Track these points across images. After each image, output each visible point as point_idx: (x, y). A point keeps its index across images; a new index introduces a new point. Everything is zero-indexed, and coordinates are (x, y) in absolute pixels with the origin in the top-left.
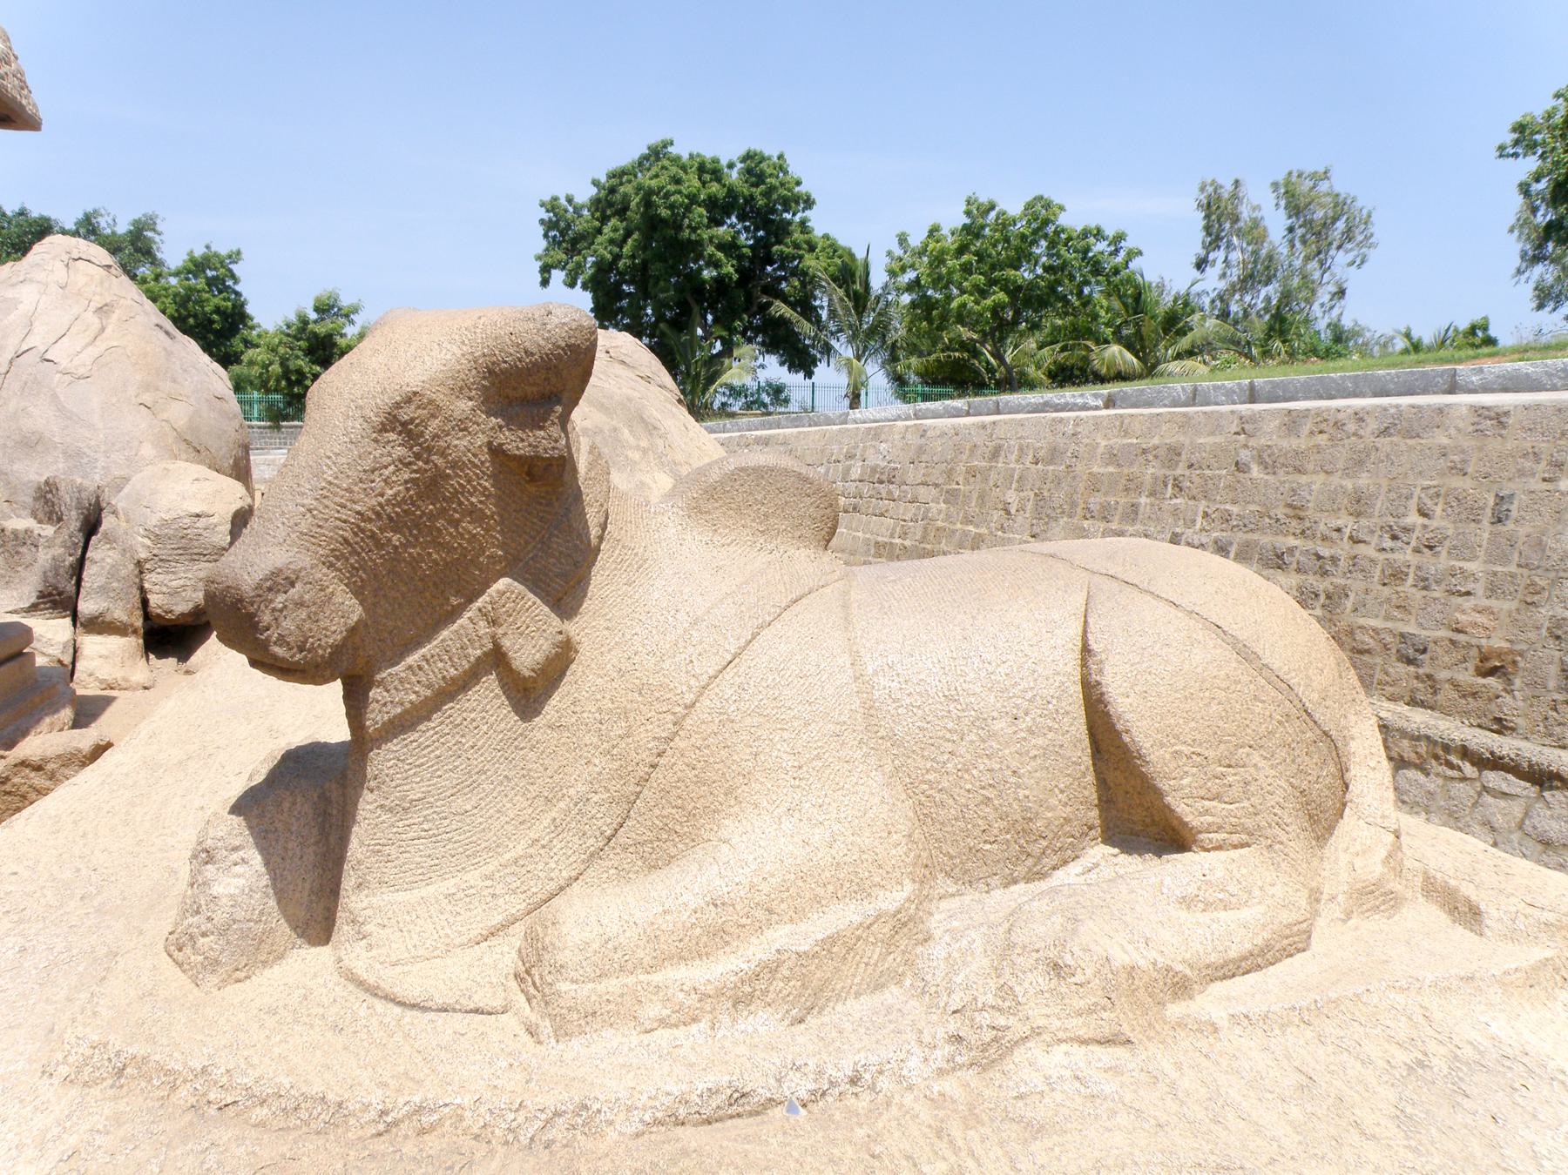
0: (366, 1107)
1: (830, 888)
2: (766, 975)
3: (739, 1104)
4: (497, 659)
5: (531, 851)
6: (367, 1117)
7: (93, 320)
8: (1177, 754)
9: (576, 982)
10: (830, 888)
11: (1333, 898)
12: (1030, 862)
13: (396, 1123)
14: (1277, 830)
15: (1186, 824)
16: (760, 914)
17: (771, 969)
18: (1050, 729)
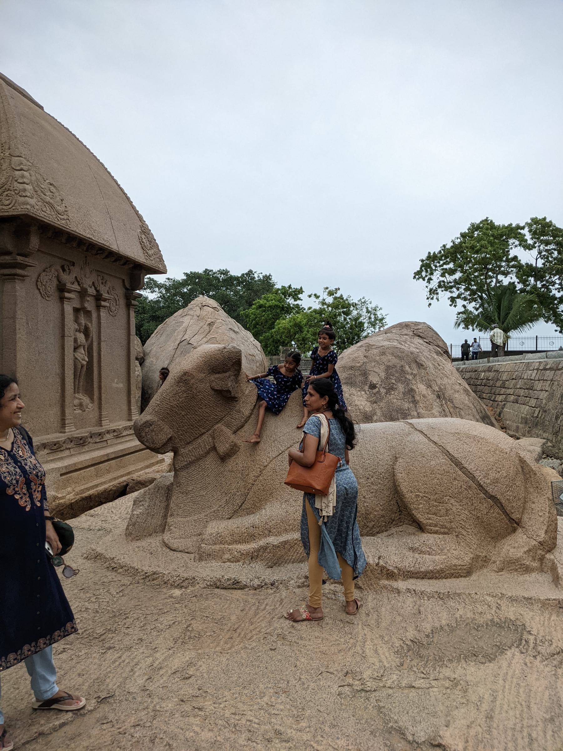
0: (143, 571)
1: (291, 527)
2: (262, 550)
3: (236, 585)
4: (214, 448)
5: (219, 509)
6: (142, 573)
7: (206, 327)
8: (417, 496)
9: (206, 544)
10: (291, 527)
11: (494, 562)
12: (368, 529)
13: (148, 576)
14: (461, 530)
15: (421, 522)
16: (266, 532)
17: (264, 548)
18: (380, 483)
